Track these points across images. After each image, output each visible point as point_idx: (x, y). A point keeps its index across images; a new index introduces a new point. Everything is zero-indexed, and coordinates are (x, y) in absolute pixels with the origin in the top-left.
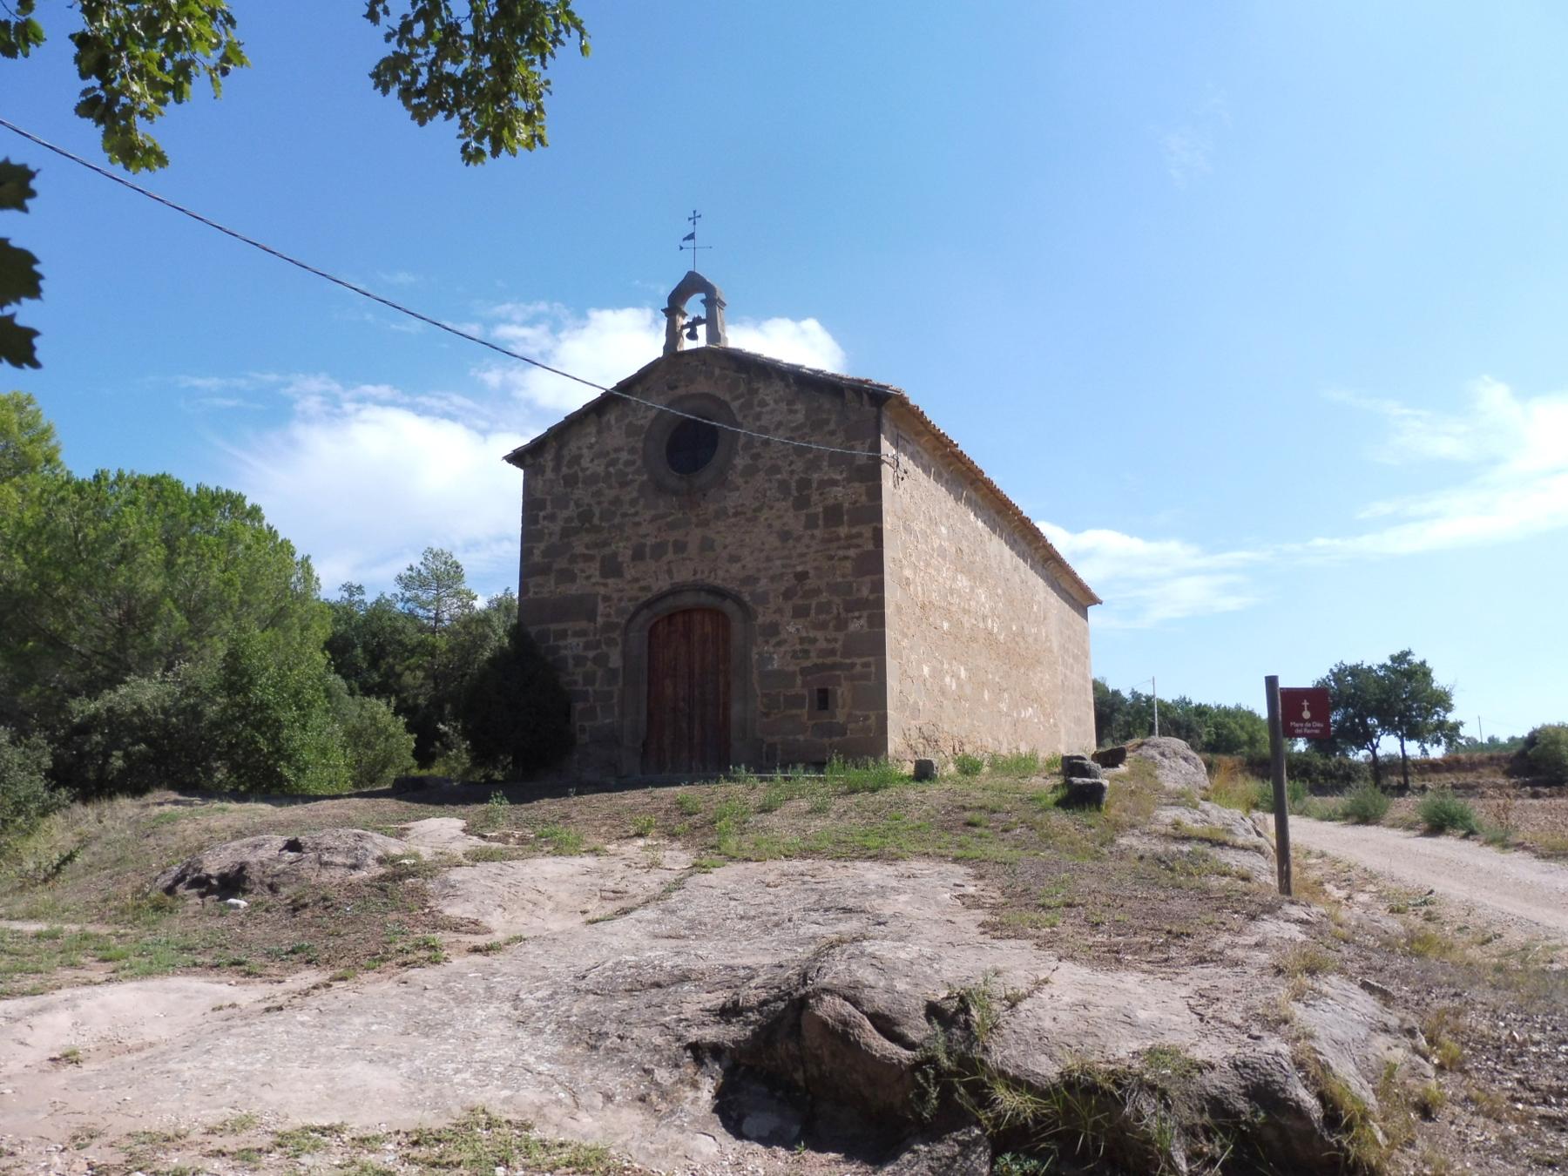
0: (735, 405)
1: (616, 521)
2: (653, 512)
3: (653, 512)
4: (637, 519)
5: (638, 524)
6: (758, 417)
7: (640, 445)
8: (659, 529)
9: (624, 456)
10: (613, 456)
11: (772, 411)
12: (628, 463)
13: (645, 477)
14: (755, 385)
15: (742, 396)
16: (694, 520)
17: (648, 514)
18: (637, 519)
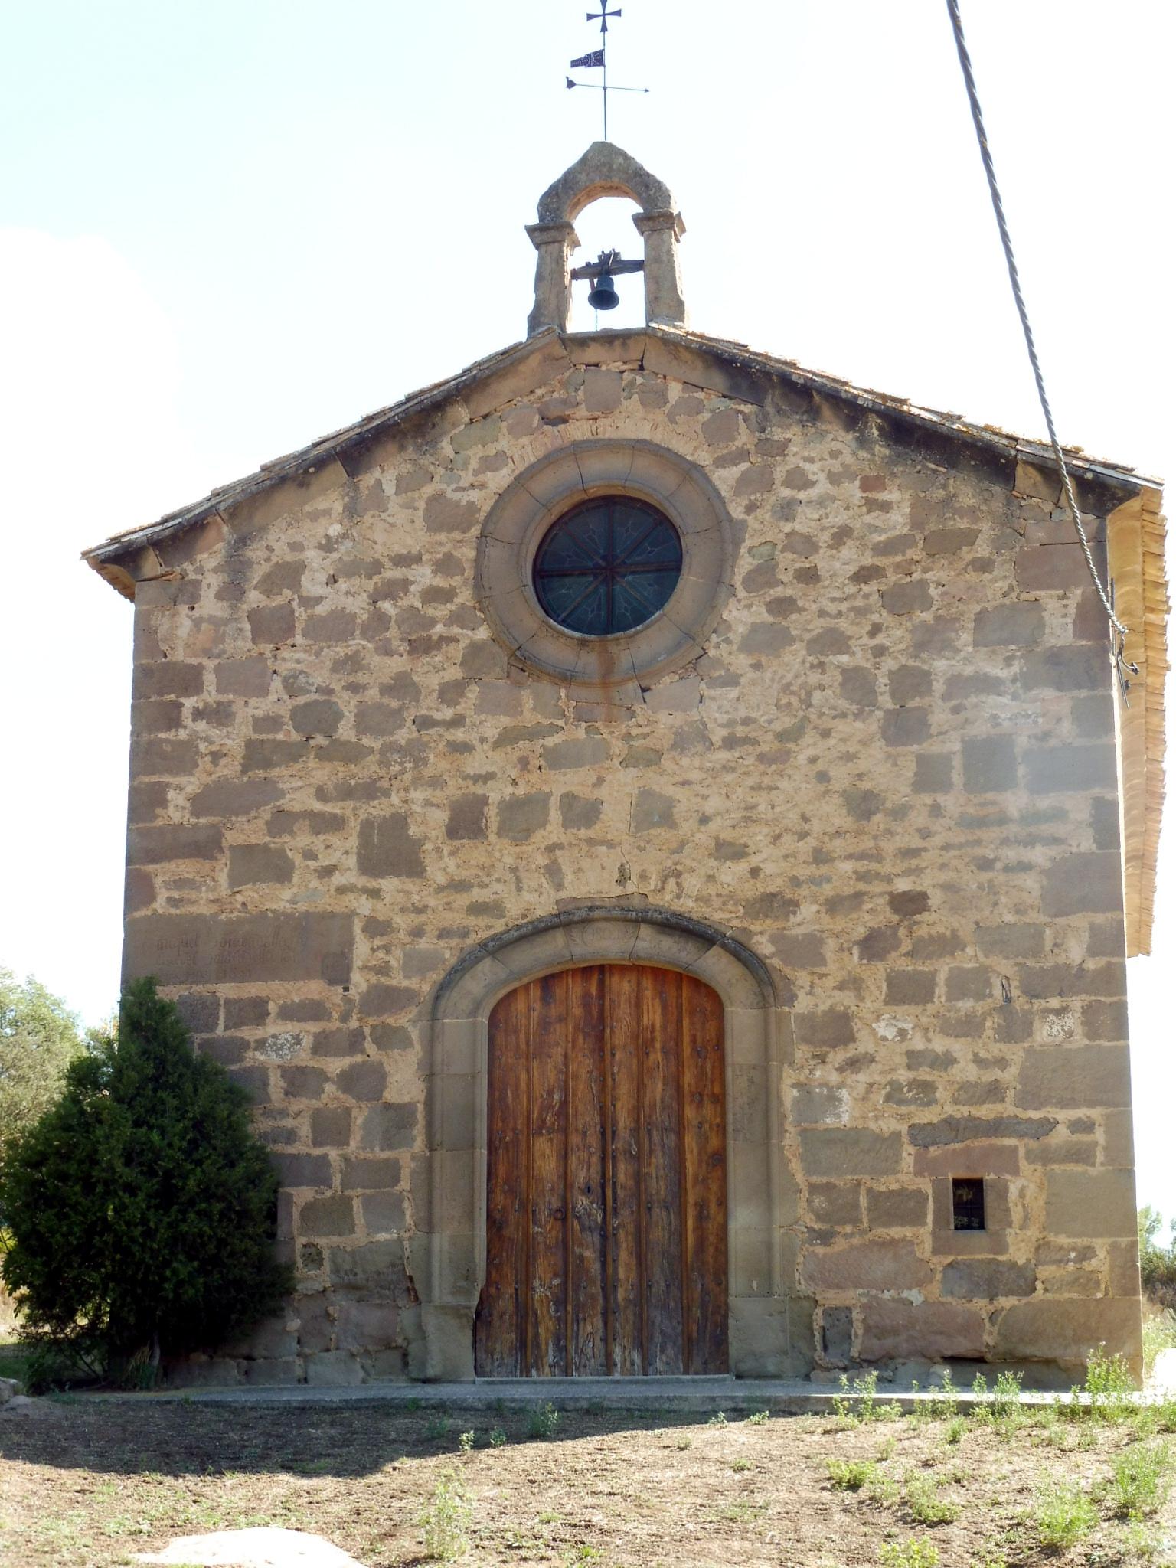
0: (725, 478)
1: (404, 735)
2: (505, 721)
3: (505, 721)
4: (459, 735)
5: (466, 748)
6: (786, 511)
7: (468, 553)
8: (524, 763)
9: (423, 576)
10: (391, 573)
11: (821, 502)
12: (433, 595)
13: (483, 633)
14: (777, 434)
15: (742, 455)
16: (618, 747)
17: (493, 726)
18: (459, 735)
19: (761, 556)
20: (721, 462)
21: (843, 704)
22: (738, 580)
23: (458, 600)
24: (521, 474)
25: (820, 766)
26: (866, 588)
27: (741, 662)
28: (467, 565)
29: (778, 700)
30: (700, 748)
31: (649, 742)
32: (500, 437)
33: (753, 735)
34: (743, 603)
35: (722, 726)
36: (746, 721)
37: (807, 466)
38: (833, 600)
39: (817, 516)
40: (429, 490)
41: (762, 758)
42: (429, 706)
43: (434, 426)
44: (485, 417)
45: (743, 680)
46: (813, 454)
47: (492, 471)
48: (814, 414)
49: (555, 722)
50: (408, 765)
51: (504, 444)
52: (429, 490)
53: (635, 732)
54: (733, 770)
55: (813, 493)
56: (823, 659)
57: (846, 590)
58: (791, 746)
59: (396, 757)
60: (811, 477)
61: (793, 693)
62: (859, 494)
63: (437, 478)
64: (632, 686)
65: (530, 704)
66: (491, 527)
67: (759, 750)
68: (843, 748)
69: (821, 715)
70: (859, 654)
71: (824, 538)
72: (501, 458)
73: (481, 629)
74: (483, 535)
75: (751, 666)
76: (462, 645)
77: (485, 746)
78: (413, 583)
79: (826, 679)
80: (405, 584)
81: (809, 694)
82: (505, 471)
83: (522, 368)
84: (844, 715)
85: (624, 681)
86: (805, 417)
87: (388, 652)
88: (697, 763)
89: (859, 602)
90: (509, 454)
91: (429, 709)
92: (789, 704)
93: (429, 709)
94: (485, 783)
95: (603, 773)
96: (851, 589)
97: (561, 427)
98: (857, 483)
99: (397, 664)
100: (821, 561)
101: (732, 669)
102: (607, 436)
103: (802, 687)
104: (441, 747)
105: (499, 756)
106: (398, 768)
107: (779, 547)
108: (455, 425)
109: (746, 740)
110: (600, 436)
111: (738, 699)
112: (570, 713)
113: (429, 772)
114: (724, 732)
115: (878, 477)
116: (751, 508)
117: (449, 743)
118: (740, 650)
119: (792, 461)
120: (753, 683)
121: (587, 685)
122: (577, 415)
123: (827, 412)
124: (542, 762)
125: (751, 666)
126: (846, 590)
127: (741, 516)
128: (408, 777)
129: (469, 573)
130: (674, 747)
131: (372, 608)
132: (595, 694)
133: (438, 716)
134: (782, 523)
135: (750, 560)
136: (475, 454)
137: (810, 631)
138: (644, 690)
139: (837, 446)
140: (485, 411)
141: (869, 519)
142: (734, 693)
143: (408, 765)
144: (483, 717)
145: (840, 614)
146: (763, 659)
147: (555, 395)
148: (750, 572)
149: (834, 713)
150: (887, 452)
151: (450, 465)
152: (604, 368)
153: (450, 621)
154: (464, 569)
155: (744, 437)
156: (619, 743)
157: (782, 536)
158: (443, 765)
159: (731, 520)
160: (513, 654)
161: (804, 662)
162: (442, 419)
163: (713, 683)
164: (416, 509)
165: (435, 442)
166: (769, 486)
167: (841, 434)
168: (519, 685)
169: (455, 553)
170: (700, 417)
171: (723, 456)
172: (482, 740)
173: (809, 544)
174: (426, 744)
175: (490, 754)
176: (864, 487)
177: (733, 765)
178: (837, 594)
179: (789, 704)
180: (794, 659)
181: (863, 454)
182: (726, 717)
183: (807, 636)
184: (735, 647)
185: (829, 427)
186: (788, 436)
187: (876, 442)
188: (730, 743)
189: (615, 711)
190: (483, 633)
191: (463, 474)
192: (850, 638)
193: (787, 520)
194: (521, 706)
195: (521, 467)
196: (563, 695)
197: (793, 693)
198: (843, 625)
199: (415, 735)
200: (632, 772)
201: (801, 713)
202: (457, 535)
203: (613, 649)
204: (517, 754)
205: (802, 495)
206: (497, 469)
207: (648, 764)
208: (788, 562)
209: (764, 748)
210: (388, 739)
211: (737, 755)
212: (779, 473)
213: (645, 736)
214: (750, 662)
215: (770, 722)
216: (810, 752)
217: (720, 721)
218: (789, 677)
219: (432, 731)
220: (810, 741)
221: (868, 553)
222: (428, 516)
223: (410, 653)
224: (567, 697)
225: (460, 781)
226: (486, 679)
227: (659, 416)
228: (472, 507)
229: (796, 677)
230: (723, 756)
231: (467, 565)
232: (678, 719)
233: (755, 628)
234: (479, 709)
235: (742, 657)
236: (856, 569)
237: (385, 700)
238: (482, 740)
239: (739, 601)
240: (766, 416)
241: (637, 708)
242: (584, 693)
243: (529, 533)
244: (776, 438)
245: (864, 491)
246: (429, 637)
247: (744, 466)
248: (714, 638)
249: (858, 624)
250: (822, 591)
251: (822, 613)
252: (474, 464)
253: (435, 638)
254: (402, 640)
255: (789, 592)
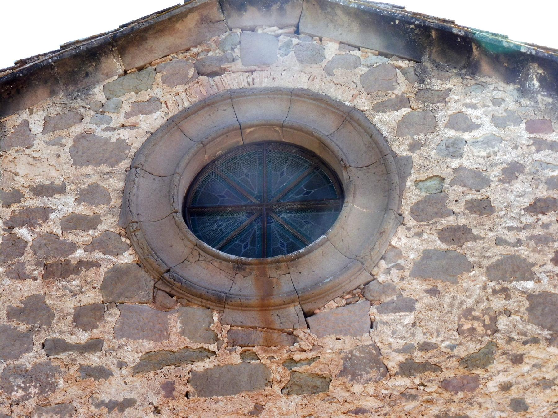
0: (386, 122)
1: (30, 359)
2: (148, 345)
3: (148, 345)
4: (94, 359)
5: (102, 373)
6: (453, 149)
7: (116, 184)
8: (169, 389)
9: (66, 205)
10: (31, 202)
11: (487, 142)
12: (73, 222)
13: (127, 258)
14: (437, 84)
15: (402, 102)
16: (278, 372)
17: (132, 353)
18: (94, 359)
19: (428, 189)
20: (380, 107)
21: (533, 329)
22: (406, 210)
23: (102, 227)
24: (174, 116)
25: (514, 393)
26: (544, 219)
27: (415, 288)
28: (114, 195)
29: (460, 326)
30: (373, 374)
31: (315, 368)
32: (154, 86)
33: (434, 360)
34: (413, 231)
35: (399, 351)
36: (425, 347)
37: (470, 111)
38: (510, 229)
39: (484, 154)
40: (77, 129)
41: (445, 385)
42: (62, 330)
43: (87, 75)
44: (140, 69)
45: (418, 306)
46: (475, 101)
47: (144, 114)
48: (472, 69)
49: (206, 346)
50: (32, 390)
51: (158, 91)
52: (77, 129)
53: (298, 356)
54: (414, 397)
55: (478, 134)
56: (505, 285)
57: (523, 219)
58: (478, 372)
59: (19, 381)
60: (474, 120)
61: (475, 318)
62: (526, 135)
63: (87, 119)
64: (294, 310)
65: (177, 328)
66: (142, 159)
67: (442, 376)
68: (538, 374)
69: (510, 340)
70: (545, 280)
71: (495, 173)
72: (155, 103)
73: (126, 254)
74: (133, 166)
75: (427, 291)
76: (103, 269)
77: (124, 372)
78: (53, 211)
79: (511, 305)
80: (45, 212)
81: (494, 320)
82: (158, 114)
83: (179, 26)
84: (535, 341)
85: (286, 304)
86: (463, 72)
87: (21, 276)
88: (371, 390)
89: (538, 231)
90: (163, 99)
91: (62, 332)
92: (473, 330)
93: (62, 332)
94: (122, 411)
95: (262, 401)
96: (528, 219)
97: (217, 78)
98: (523, 125)
99: (28, 288)
100: (494, 193)
101: (405, 294)
102: (263, 85)
103: (484, 312)
104: (72, 371)
105: (139, 382)
106: (20, 393)
107: (447, 181)
108: (108, 76)
109: (425, 367)
110: (256, 85)
111: (414, 325)
112: (223, 336)
113: (57, 398)
114: (401, 358)
115: (543, 121)
116: (414, 147)
117: (82, 368)
118: (413, 275)
119: (454, 108)
120: (430, 308)
121: (244, 307)
122: (234, 68)
123: (485, 67)
124: (190, 388)
125: (427, 291)
126: (523, 219)
127: (405, 154)
128: (31, 403)
129: (116, 201)
130: (343, 373)
131: (7, 234)
132: (252, 318)
133: (71, 340)
134: (449, 160)
135: (417, 192)
136: (128, 100)
137: (488, 258)
138: (307, 315)
139: (498, 95)
140: (140, 64)
141: (539, 156)
142: (409, 318)
143: (32, 390)
144: (123, 341)
145: (519, 242)
146: (440, 285)
147: (211, 54)
148: (418, 203)
149: (524, 338)
150: (550, 100)
151: (101, 109)
152: (260, 31)
153: (91, 247)
154: (110, 199)
155: (403, 87)
156: (280, 369)
157: (450, 171)
158: (74, 391)
159: (395, 156)
160: (161, 278)
161: (485, 288)
162: (96, 69)
163: (384, 308)
164: (63, 145)
165: (87, 89)
166: (433, 127)
167: (502, 85)
168: (166, 309)
169: (101, 184)
170: (357, 70)
171: (383, 103)
172: (121, 365)
173: (480, 179)
174: (56, 369)
175: (129, 379)
176: (531, 127)
177: (413, 392)
178: (515, 224)
179: (473, 330)
180: (473, 286)
181: (525, 102)
182: (402, 342)
183: (486, 263)
184: (407, 273)
185: (488, 80)
186: (448, 86)
187: (538, 92)
188: (408, 369)
189: (275, 335)
190: (127, 258)
191: (113, 116)
192: (533, 265)
193: (453, 157)
194: (166, 330)
195: (174, 111)
196: (216, 318)
197: (475, 318)
198: (524, 252)
199: (44, 359)
200: (296, 399)
201: (487, 339)
202: (105, 168)
203: (273, 273)
204: (161, 380)
205: (467, 136)
206: (150, 113)
207: (314, 390)
208: (457, 196)
209: (448, 374)
210: (12, 363)
211: (417, 381)
212: (442, 117)
213: (309, 361)
214: (425, 287)
215: (452, 347)
216: (502, 378)
217: (394, 346)
218: (470, 302)
219: (62, 356)
220: (501, 367)
221: (543, 187)
222: (74, 151)
223: (44, 277)
224: (220, 320)
225: (93, 408)
226: (129, 304)
227: (316, 70)
228: (122, 144)
229: (478, 302)
230: (402, 382)
231: (114, 195)
232: (347, 344)
233: (427, 255)
234: (119, 333)
235: (415, 282)
236: (532, 201)
237: (13, 324)
238: (121, 365)
239: (409, 229)
240: (424, 70)
241: (300, 332)
242: (239, 316)
243: (183, 165)
244: (436, 88)
245: (531, 133)
246: (68, 262)
247: (405, 111)
248: (383, 264)
249: (539, 252)
250: (498, 221)
251: (499, 241)
252: (126, 108)
253: (74, 262)
254: (37, 264)
255: (462, 221)
